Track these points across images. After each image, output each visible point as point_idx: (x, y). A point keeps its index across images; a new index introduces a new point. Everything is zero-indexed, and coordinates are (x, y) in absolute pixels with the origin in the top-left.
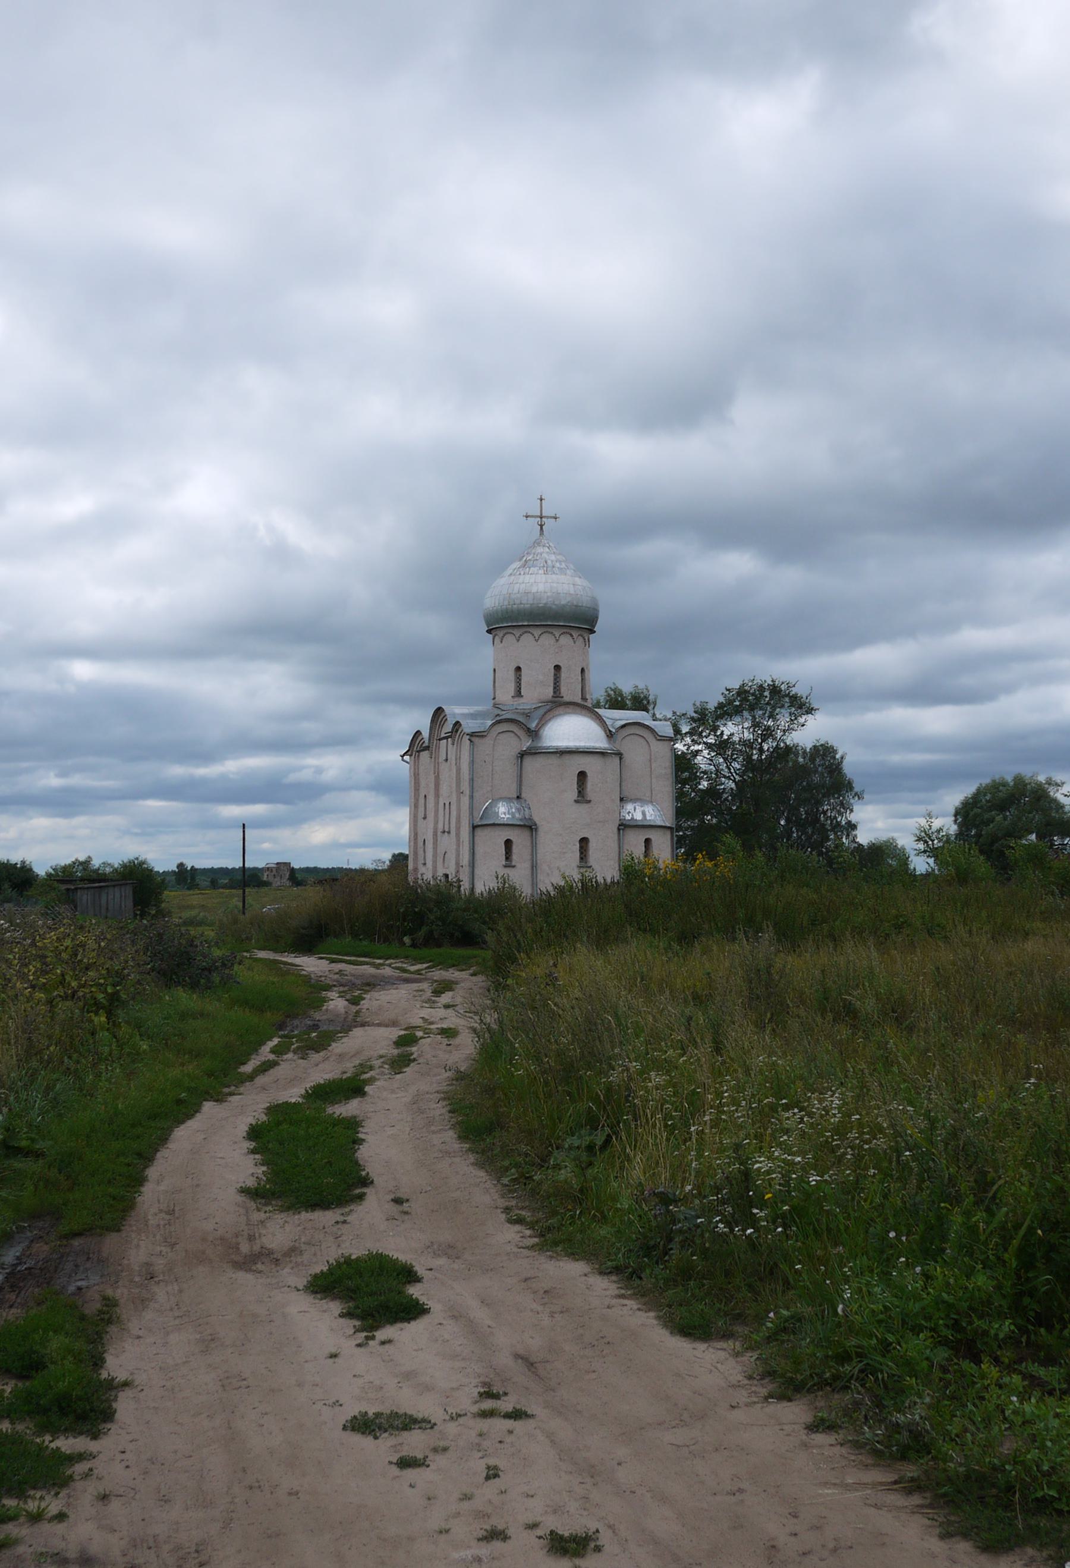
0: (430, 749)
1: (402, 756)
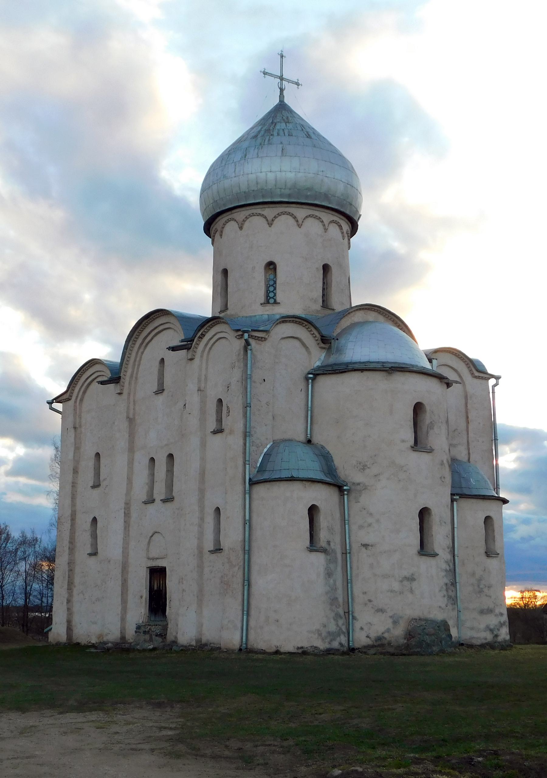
0: (122, 380)
1: (50, 403)
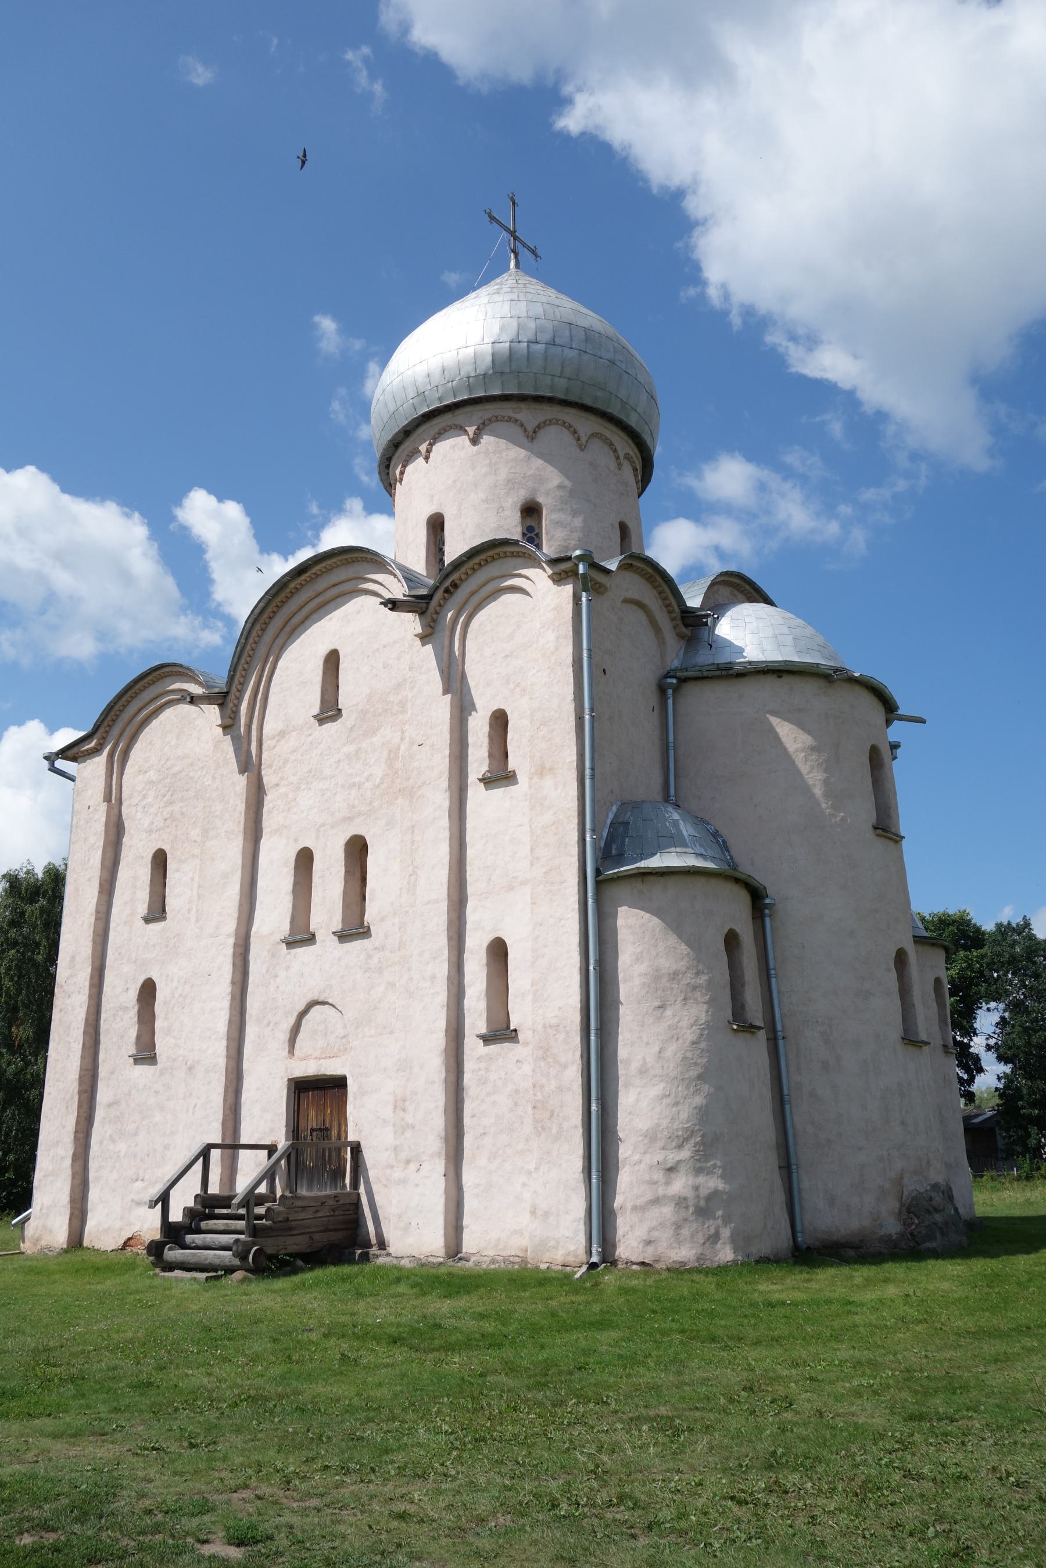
1: (50, 758)
